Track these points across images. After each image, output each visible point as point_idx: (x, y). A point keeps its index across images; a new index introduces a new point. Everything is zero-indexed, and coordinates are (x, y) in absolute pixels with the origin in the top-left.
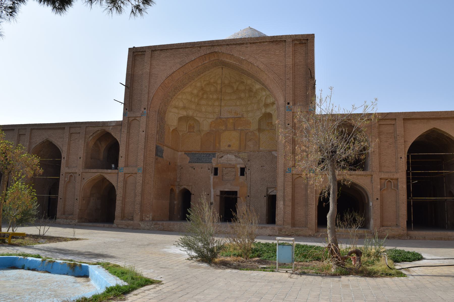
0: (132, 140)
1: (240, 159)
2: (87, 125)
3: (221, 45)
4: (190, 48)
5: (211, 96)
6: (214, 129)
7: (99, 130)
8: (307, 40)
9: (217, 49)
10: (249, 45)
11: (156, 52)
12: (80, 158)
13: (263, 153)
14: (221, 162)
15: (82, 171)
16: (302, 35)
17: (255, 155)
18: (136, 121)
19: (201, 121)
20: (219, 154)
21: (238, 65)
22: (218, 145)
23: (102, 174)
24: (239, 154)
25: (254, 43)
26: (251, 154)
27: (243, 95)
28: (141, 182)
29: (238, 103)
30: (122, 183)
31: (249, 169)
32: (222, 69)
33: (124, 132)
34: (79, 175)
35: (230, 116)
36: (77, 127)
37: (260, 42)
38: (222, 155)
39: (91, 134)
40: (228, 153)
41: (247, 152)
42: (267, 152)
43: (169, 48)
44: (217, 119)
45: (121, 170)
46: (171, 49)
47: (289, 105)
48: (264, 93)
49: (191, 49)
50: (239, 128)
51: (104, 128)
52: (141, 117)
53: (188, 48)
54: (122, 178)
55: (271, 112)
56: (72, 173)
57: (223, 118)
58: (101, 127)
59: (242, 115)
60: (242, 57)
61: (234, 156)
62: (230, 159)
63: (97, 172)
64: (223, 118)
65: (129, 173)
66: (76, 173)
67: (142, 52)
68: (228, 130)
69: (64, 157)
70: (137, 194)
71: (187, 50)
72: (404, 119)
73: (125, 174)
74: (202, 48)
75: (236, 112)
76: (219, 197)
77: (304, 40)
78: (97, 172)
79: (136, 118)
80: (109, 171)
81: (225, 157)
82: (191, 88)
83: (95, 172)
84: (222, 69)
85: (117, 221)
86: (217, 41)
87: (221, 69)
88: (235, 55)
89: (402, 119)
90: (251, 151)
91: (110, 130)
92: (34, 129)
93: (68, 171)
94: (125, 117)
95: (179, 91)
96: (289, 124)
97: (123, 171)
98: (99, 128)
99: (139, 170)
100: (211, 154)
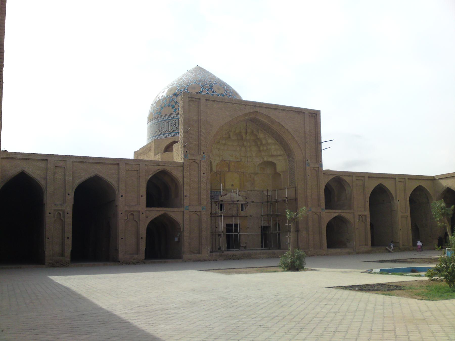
0: (192, 180)
1: (241, 197)
2: (147, 164)
3: (261, 107)
4: (238, 104)
6: (220, 170)
7: (159, 169)
8: (317, 114)
9: (258, 110)
10: (281, 111)
11: (209, 102)
12: (142, 196)
14: (226, 199)
15: (145, 209)
16: (314, 110)
18: (194, 163)
21: (270, 125)
23: (166, 212)
25: (283, 110)
28: (206, 219)
30: (188, 220)
31: (248, 205)
32: (246, 123)
33: (186, 173)
34: (143, 213)
35: (232, 159)
36: (134, 164)
37: (288, 110)
38: (226, 193)
39: (152, 172)
40: (231, 191)
43: (221, 100)
44: (222, 160)
45: (187, 208)
46: (222, 102)
47: (307, 162)
48: (273, 147)
49: (238, 105)
50: (239, 171)
51: (165, 167)
52: (200, 160)
53: (236, 104)
54: (188, 215)
55: (275, 162)
56: (134, 211)
57: (227, 161)
58: (162, 167)
59: (241, 159)
60: (276, 120)
61: (235, 194)
62: (235, 197)
63: (161, 211)
64: (227, 161)
65: (193, 211)
66: (139, 212)
67: (195, 98)
68: (231, 172)
69: (121, 195)
70: (203, 230)
71: (235, 105)
72: (369, 177)
73: (190, 211)
74: (247, 106)
76: (226, 229)
77: (314, 114)
78: (161, 211)
79: (195, 161)
80: (175, 209)
81: (229, 194)
83: (160, 211)
84: (246, 123)
85: (186, 256)
86: (259, 103)
87: (246, 122)
88: (272, 117)
89: (367, 177)
90: (249, 191)
92: (76, 162)
93: (128, 209)
94: (186, 159)
96: (308, 176)
97: (188, 210)
99: (204, 208)
100: (218, 192)
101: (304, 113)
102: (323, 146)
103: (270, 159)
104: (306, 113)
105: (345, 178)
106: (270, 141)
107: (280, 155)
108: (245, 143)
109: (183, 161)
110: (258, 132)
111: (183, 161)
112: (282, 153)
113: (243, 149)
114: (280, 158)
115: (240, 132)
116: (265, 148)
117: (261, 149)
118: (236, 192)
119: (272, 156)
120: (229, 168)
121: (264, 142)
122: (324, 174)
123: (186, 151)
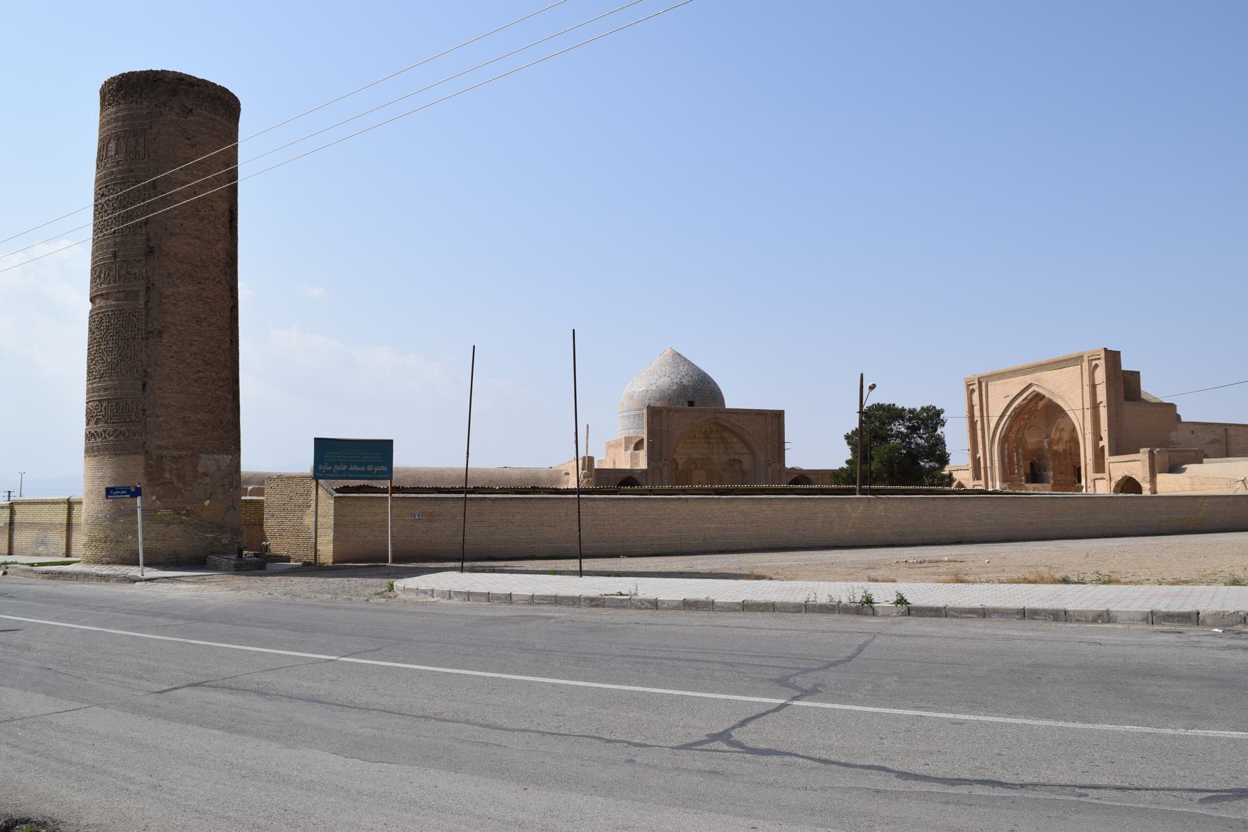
9: (719, 415)
16: (777, 411)
51: (630, 474)
55: (741, 459)
91: (636, 476)
98: (627, 475)
101: (766, 414)
102: (787, 446)
103: (737, 457)
104: (769, 414)
105: (809, 476)
106: (734, 440)
107: (746, 454)
108: (712, 441)
109: (646, 468)
111: (646, 468)
114: (746, 456)
115: (706, 431)
116: (731, 446)
119: (739, 454)
120: (696, 466)
121: (729, 441)
122: (787, 473)
123: (650, 459)
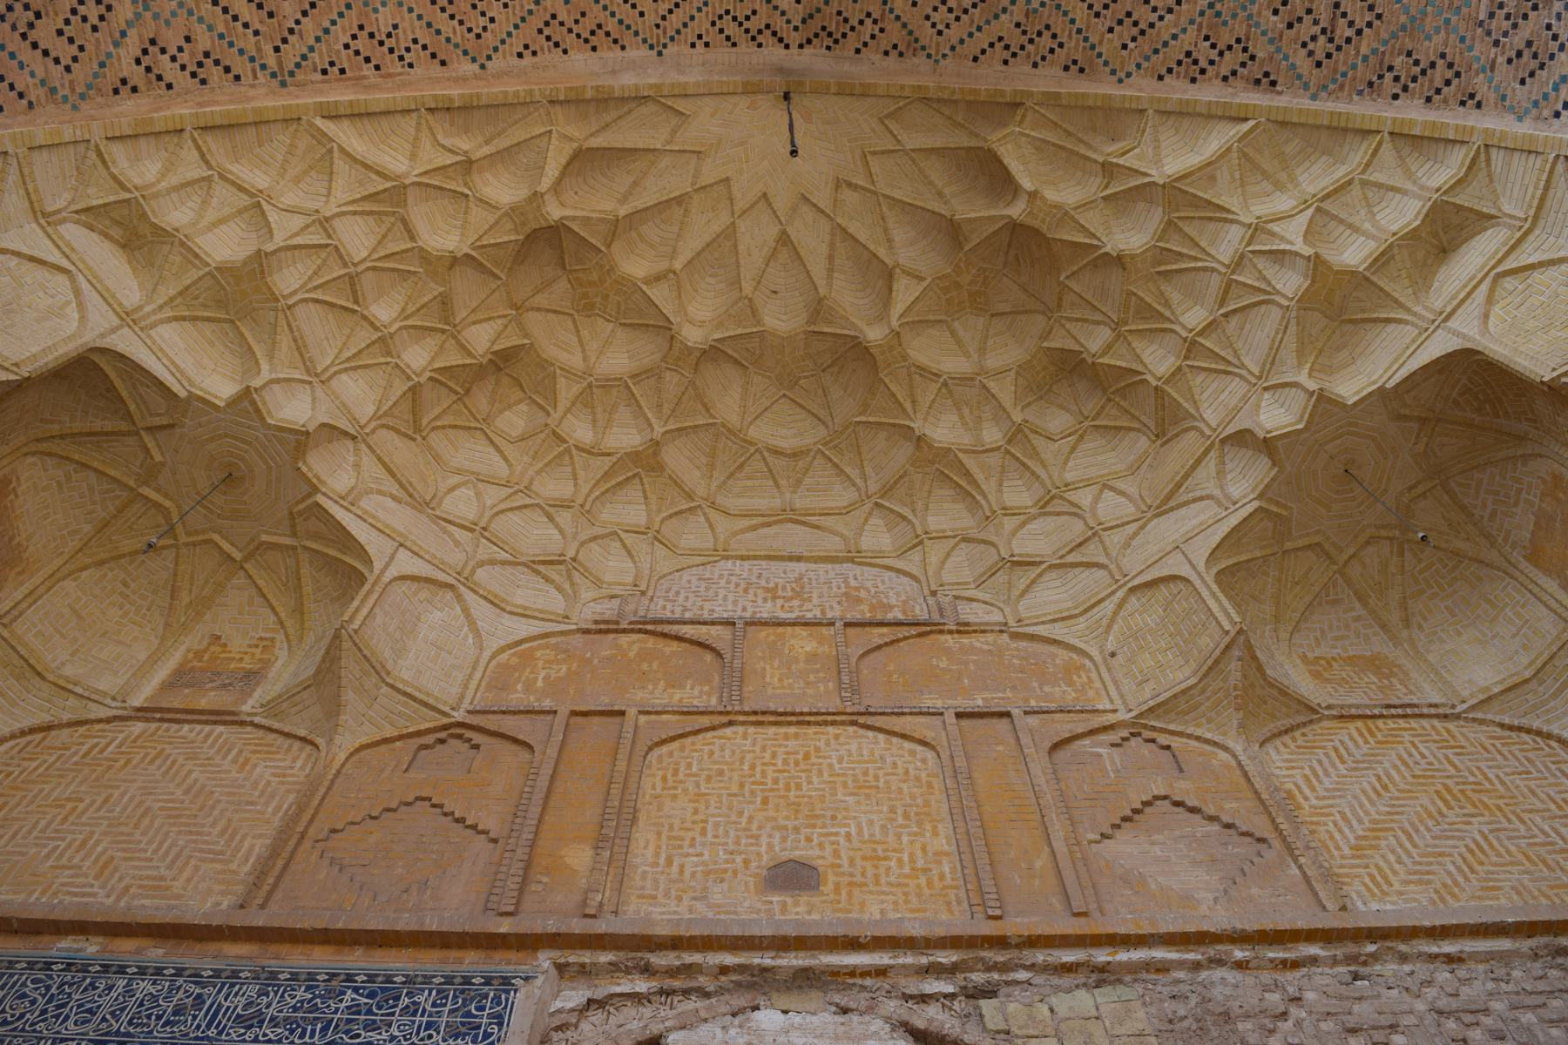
5: (580, 431)
13: (1443, 975)
17: (1295, 1012)
19: (393, 572)
20: (573, 997)
22: (579, 857)
24: (986, 1005)
26: (1217, 993)
27: (943, 431)
29: (878, 537)
41: (1133, 968)
42: (1504, 957)
61: (877, 1025)
75: (863, 594)
82: (413, 157)
95: (282, 79)
110: (1000, 181)
112: (1440, 174)
113: (945, 515)
117: (1158, 360)
118: (892, 1006)
